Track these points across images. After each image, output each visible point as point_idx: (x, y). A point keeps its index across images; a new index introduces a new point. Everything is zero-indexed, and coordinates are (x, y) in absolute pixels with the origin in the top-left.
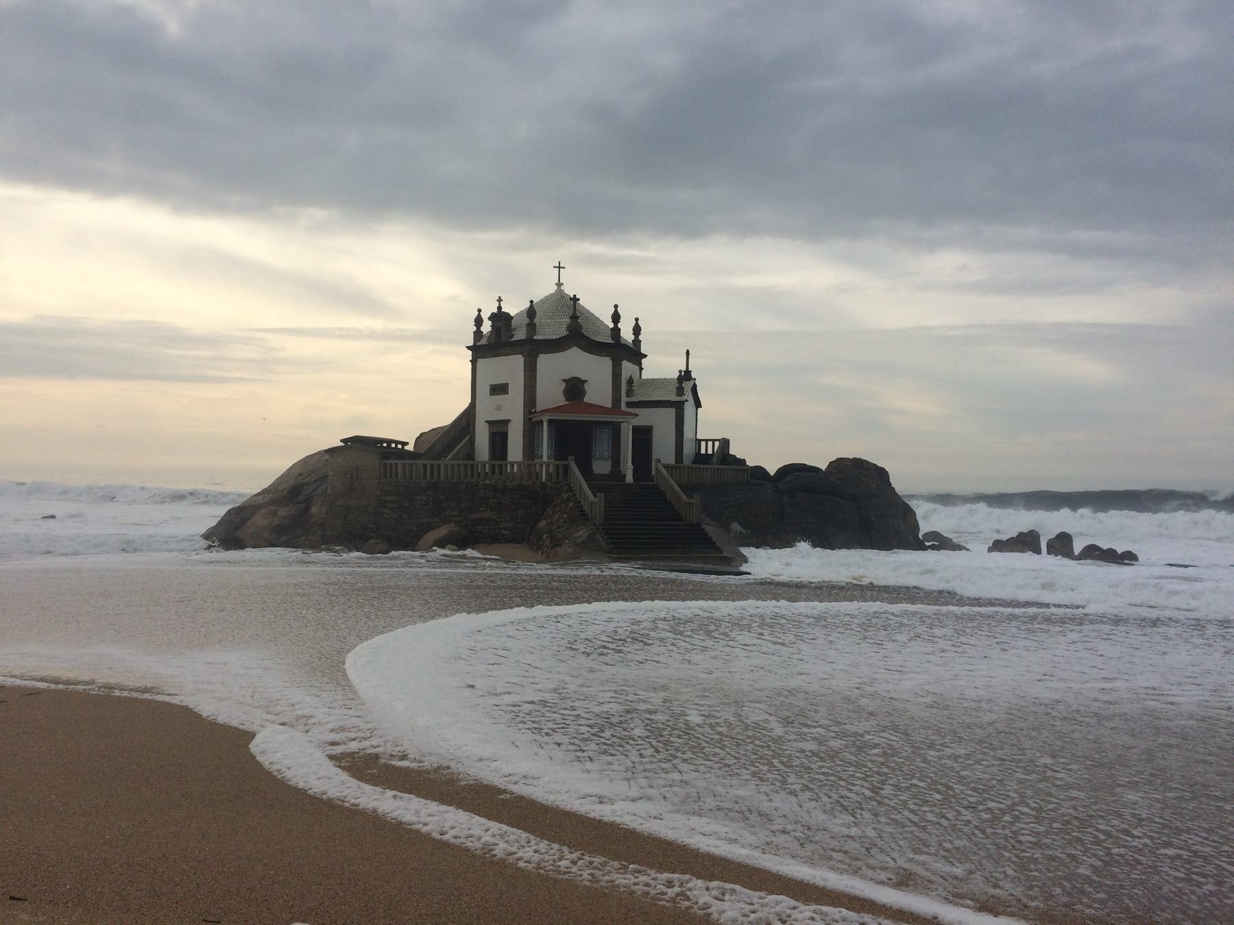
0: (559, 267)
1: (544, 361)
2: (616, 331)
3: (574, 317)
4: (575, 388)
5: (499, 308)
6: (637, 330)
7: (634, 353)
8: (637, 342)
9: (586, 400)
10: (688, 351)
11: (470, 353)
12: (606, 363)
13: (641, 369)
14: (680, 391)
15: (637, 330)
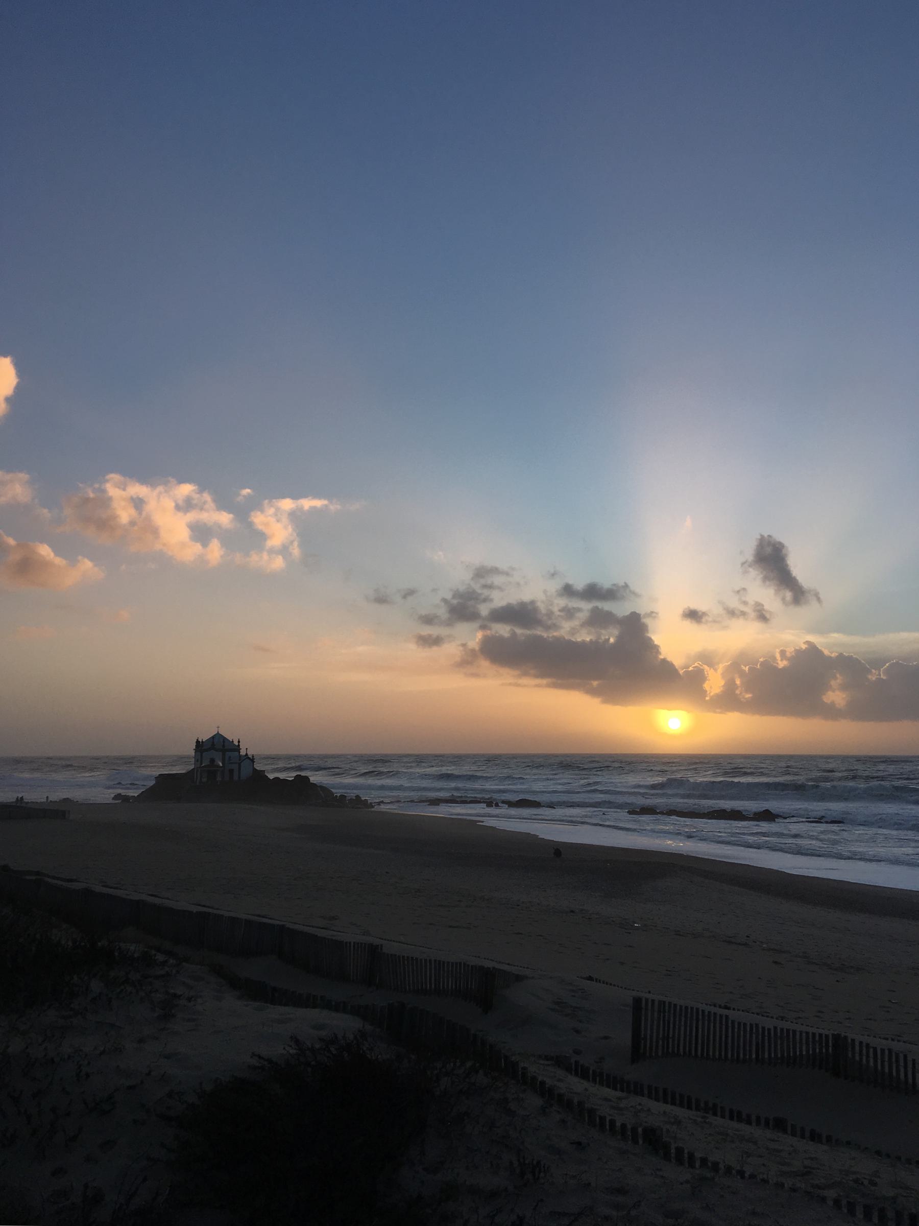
0: (218, 727)
1: (204, 754)
2: (224, 746)
3: (213, 742)
4: (212, 761)
5: (197, 740)
6: (239, 742)
7: (237, 749)
8: (239, 745)
9: (215, 763)
10: (247, 749)
11: (194, 751)
12: (221, 753)
13: (240, 752)
14: (240, 760)
15: (239, 742)
